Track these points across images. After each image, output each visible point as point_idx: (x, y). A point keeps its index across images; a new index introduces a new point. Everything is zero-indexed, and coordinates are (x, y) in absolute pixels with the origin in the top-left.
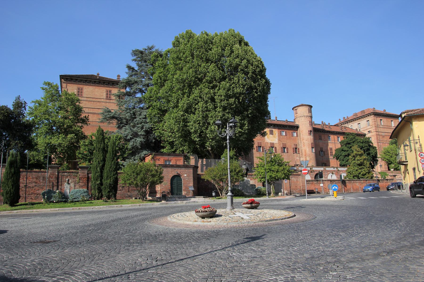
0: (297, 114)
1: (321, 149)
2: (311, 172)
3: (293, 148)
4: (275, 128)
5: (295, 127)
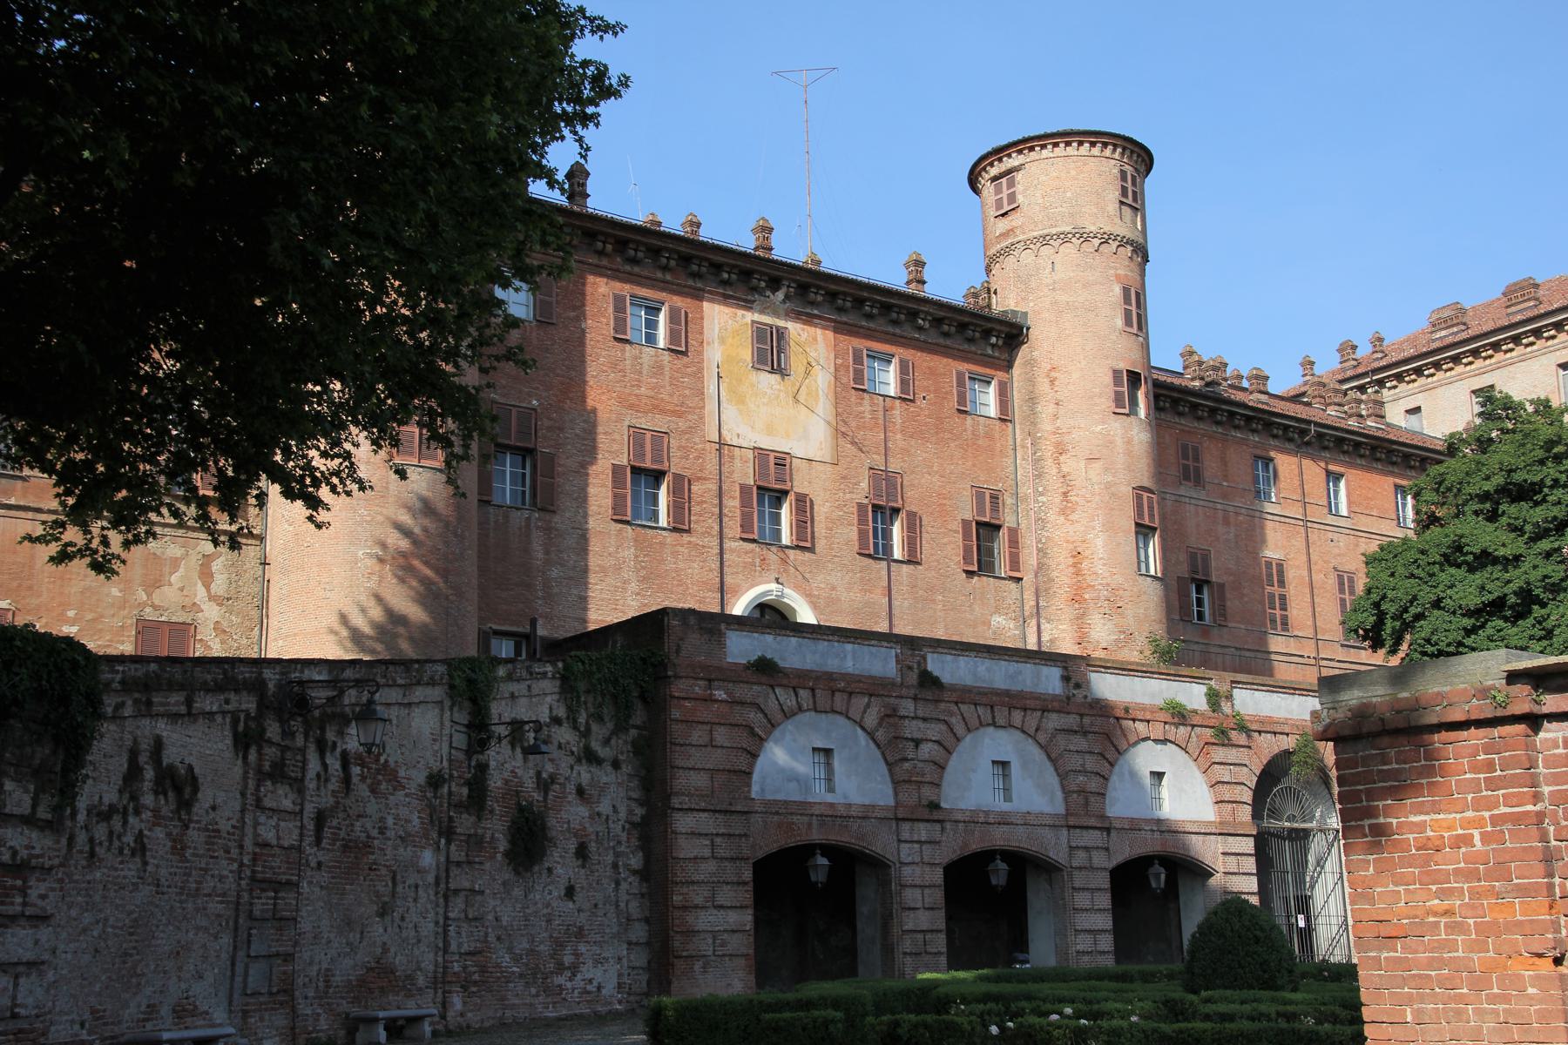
0: (1014, 220)
1: (1193, 557)
2: (1222, 737)
3: (965, 523)
4: (808, 319)
5: (987, 333)
